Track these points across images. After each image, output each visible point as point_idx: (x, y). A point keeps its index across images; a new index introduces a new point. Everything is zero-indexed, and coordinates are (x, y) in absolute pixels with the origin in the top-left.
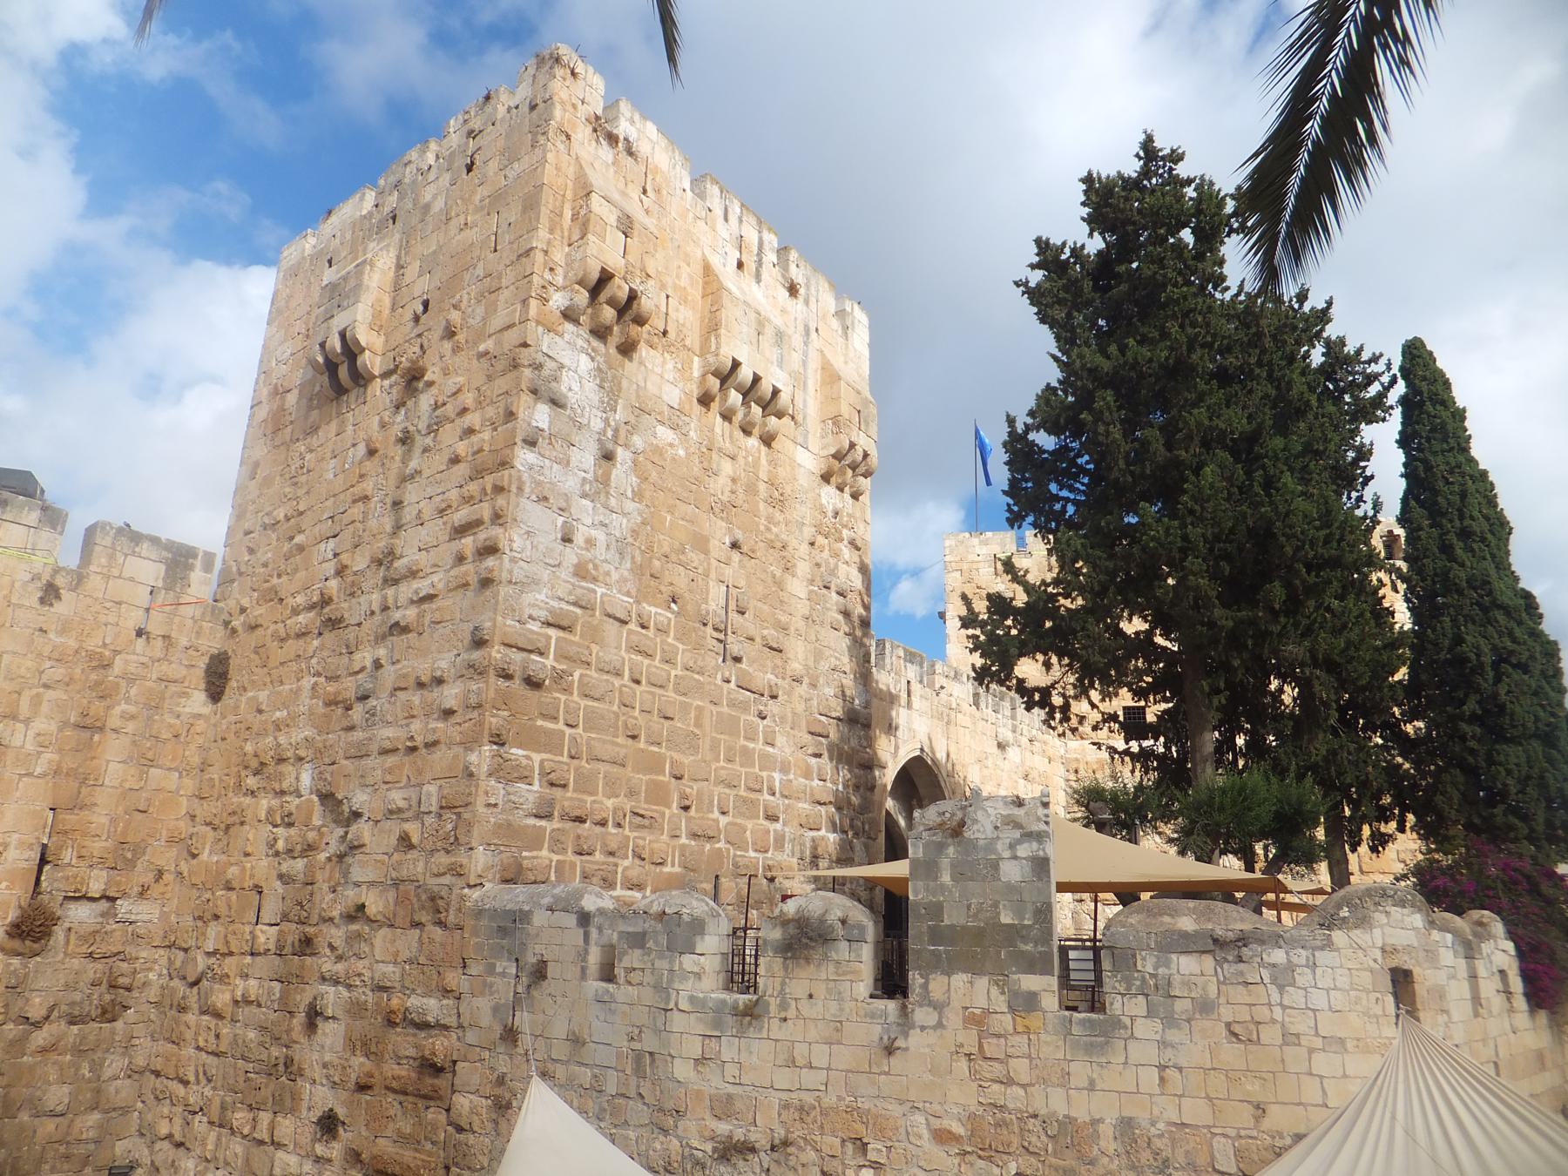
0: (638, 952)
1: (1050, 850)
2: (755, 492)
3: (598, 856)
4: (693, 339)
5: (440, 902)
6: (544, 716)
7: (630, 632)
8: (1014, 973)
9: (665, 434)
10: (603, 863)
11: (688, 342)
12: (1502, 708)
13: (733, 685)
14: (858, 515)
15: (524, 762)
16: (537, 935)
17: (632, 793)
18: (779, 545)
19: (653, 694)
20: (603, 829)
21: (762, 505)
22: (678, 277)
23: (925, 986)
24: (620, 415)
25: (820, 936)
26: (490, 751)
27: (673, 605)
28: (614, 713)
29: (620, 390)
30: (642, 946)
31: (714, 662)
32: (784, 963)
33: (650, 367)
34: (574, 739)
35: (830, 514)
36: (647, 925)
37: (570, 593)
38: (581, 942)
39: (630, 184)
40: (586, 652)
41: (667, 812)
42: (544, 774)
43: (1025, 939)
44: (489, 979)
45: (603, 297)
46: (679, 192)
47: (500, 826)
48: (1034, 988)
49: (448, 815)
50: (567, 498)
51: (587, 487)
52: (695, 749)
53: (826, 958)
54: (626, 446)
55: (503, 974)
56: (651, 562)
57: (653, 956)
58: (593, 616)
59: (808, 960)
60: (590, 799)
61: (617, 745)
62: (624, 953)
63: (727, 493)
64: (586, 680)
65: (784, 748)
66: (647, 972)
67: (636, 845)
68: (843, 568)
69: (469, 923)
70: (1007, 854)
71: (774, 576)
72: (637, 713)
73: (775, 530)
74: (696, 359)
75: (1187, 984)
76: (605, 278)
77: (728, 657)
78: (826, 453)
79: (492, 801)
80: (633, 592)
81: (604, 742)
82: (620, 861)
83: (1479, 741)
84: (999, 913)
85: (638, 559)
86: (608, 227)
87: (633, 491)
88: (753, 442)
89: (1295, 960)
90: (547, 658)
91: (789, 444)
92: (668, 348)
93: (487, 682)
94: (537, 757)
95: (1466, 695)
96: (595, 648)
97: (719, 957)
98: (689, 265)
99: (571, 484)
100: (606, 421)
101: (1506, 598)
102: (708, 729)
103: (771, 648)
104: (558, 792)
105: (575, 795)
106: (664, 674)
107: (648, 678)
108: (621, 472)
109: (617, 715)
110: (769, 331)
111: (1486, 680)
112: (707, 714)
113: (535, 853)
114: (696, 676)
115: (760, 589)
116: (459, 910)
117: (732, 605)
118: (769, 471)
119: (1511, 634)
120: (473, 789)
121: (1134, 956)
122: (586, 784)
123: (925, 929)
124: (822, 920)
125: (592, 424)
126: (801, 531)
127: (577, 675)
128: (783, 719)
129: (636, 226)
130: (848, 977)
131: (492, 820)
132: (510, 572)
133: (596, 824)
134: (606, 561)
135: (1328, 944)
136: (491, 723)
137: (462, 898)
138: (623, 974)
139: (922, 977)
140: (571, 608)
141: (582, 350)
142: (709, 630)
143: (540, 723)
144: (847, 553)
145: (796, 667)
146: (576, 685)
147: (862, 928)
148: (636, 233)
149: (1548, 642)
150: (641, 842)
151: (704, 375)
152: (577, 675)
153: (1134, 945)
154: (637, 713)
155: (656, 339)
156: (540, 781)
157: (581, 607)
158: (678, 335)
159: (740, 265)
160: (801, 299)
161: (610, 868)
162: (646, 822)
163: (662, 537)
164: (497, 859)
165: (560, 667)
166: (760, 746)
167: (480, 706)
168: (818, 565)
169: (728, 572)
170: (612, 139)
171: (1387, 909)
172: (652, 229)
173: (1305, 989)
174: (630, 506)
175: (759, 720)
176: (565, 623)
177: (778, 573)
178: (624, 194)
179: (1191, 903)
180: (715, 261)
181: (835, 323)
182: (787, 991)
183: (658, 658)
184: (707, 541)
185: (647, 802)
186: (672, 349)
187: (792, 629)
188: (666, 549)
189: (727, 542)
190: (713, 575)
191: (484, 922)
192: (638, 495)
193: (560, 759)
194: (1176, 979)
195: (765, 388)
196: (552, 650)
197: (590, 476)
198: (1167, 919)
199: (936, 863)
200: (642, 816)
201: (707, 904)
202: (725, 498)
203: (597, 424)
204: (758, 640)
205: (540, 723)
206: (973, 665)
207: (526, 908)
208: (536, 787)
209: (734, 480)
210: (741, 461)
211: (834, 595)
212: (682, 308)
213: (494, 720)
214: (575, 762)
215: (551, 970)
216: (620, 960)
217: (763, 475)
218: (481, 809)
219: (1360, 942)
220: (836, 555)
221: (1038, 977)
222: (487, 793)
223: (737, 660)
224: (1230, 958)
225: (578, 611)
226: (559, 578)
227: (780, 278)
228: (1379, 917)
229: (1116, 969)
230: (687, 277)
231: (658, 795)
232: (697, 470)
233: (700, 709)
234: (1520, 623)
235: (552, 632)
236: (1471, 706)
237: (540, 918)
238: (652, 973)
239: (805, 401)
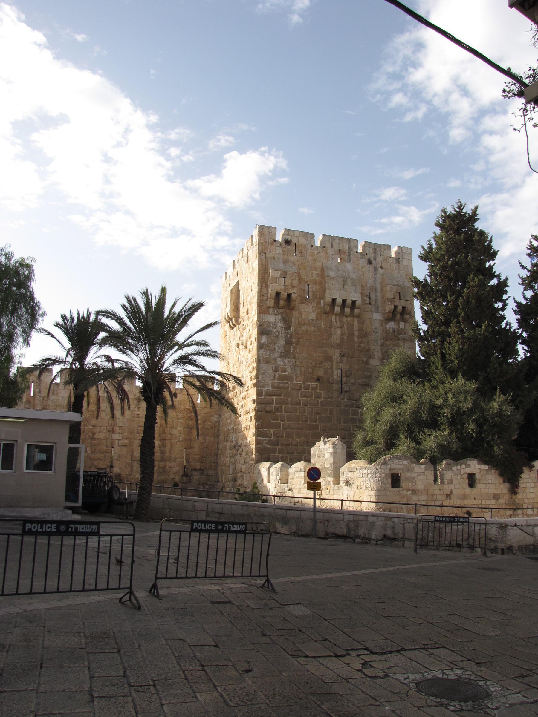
6: (273, 420)
13: (346, 400)
15: (268, 432)
20: (297, 447)
22: (312, 277)
28: (298, 415)
29: (291, 322)
42: (274, 434)
51: (282, 354)
72: (306, 414)
73: (362, 345)
80: (302, 380)
90: (273, 404)
94: (272, 431)
99: (276, 355)
103: (362, 385)
107: (310, 404)
114: (329, 400)
118: (359, 326)
142: (334, 385)
143: (272, 422)
151: (324, 305)
152: (283, 407)
154: (306, 414)
158: (313, 296)
163: (312, 361)
165: (276, 406)
183: (313, 397)
184: (332, 357)
188: (314, 364)
190: (334, 368)
195: (349, 302)
200: (311, 442)
205: (272, 422)
210: (345, 327)
217: (356, 328)
223: (346, 392)
235: (273, 397)
239: (376, 296)
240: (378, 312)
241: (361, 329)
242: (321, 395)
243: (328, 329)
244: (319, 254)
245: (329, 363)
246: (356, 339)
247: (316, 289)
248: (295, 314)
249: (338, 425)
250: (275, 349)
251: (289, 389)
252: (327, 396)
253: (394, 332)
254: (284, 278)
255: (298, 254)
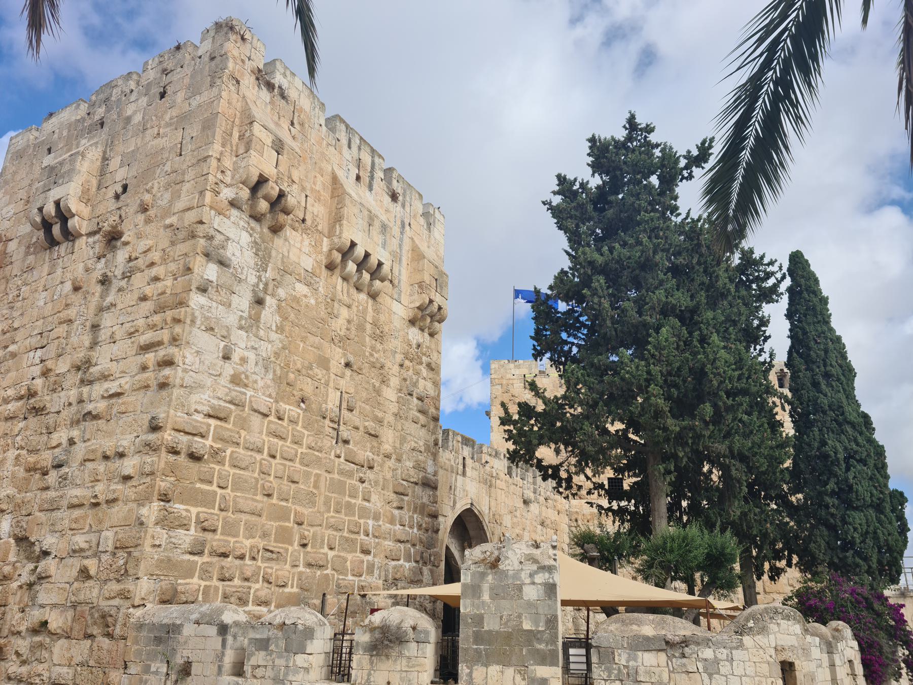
0: (263, 653)
1: (557, 578)
2: (364, 330)
3: (237, 582)
4: (323, 226)
5: (110, 619)
6: (202, 481)
7: (270, 422)
8: (532, 665)
9: (301, 289)
10: (240, 587)
11: (320, 228)
12: (850, 487)
13: (342, 460)
14: (433, 347)
15: (184, 514)
16: (186, 642)
17: (265, 535)
18: (378, 365)
19: (284, 465)
20: (242, 562)
21: (368, 339)
22: (314, 183)
23: (470, 675)
24: (270, 274)
25: (397, 639)
26: (158, 506)
27: (302, 404)
28: (255, 478)
29: (270, 257)
30: (266, 648)
31: (329, 444)
32: (370, 660)
33: (292, 243)
34: (224, 497)
35: (414, 346)
36: (270, 633)
37: (227, 395)
38: (219, 647)
39: (282, 119)
40: (237, 436)
41: (290, 548)
42: (199, 522)
43: (539, 641)
44: (144, 677)
45: (260, 194)
46: (317, 126)
47: (162, 561)
48: (545, 676)
49: (121, 554)
50: (228, 329)
51: (243, 322)
52: (313, 503)
53: (401, 654)
54: (273, 295)
55: (156, 673)
56: (287, 375)
57: (274, 656)
58: (244, 410)
59: (387, 657)
60: (232, 540)
61: (257, 501)
62: (252, 654)
63: (344, 330)
64: (235, 455)
65: (377, 503)
66: (269, 668)
67: (265, 573)
68: (422, 383)
69: (132, 634)
70: (528, 581)
71: (374, 386)
72: (272, 478)
73: (376, 355)
74: (325, 239)
75: (648, 673)
76: (262, 181)
77: (340, 440)
78: (412, 306)
79: (157, 543)
80: (274, 395)
81: (246, 499)
82: (253, 585)
83: (837, 509)
84: (522, 622)
85: (278, 372)
86: (266, 147)
87: (277, 326)
88: (363, 297)
89: (719, 656)
90: (208, 439)
91: (388, 298)
92: (305, 231)
93: (159, 457)
94: (194, 510)
95: (829, 479)
96: (243, 433)
97: (323, 656)
98: (322, 176)
99: (231, 319)
100: (259, 278)
101: (853, 417)
102: (323, 490)
103: (370, 434)
104: (209, 536)
105: (222, 537)
106: (293, 451)
107: (281, 454)
108: (269, 315)
109: (257, 480)
110: (377, 224)
111: (840, 469)
112: (322, 479)
113: (188, 581)
114: (316, 453)
115: (364, 394)
116: (125, 625)
117: (344, 405)
119: (856, 441)
120: (143, 534)
121: (613, 653)
122: (230, 529)
123: (470, 633)
124: (399, 628)
125: (249, 279)
126: (394, 357)
127: (228, 452)
128: (376, 483)
129: (286, 147)
130: (416, 669)
131: (156, 557)
132: (183, 379)
133: (236, 558)
134: (255, 373)
135: (740, 646)
136: (160, 486)
137: (128, 616)
138: (250, 671)
139: (468, 667)
140: (228, 405)
141: (244, 228)
142: (327, 422)
143: (198, 485)
144: (424, 372)
145: (387, 447)
146: (228, 459)
147: (427, 633)
148: (285, 152)
149: (879, 446)
150: (269, 571)
151: (330, 251)
152: (228, 452)
153: (613, 645)
154: (272, 478)
155: (297, 224)
156: (196, 527)
157: (235, 404)
158: (313, 222)
159: (358, 178)
160: (400, 203)
161: (245, 590)
162: (274, 556)
163: (296, 358)
164: (157, 586)
165: (216, 446)
166: (359, 501)
167: (152, 473)
168: (405, 380)
169: (342, 383)
170: (270, 86)
171: (779, 621)
172: (297, 150)
173: (726, 676)
174: (274, 336)
175: (360, 484)
176: (222, 415)
177: (377, 385)
178: (277, 124)
179: (651, 617)
180: (341, 174)
181: (422, 221)
182: (372, 679)
183: (289, 440)
185: (276, 541)
186: (308, 231)
187: (386, 422)
188: (299, 366)
189: (343, 362)
190: (331, 384)
191: (144, 633)
192: (280, 329)
193: (212, 511)
194: (641, 670)
195: (373, 261)
196: (211, 434)
197: (246, 315)
198: (635, 627)
199: (479, 586)
200: (272, 552)
201: (317, 617)
202: (342, 333)
203: (252, 280)
204: (361, 429)
205: (198, 485)
206: (508, 449)
207: (178, 622)
208: (192, 531)
209: (349, 322)
210: (354, 309)
211: (415, 399)
212: (316, 204)
213: (163, 484)
214: (224, 513)
215: (194, 670)
216: (249, 660)
217: (369, 319)
218: (148, 548)
219: (761, 644)
220: (418, 373)
221: (548, 667)
222: (153, 537)
223: (346, 442)
224: (677, 655)
225: (233, 407)
226: (219, 384)
227: (385, 189)
228: (773, 627)
229: (600, 663)
230: (321, 183)
231: (284, 536)
232: (323, 314)
233: (318, 476)
234: (861, 433)
235: (212, 422)
236: (831, 486)
237: (189, 630)
238: (273, 669)
240: (400, 302)
241: (375, 324)
242: (303, 438)
243: (329, 300)
244: (330, 147)
245: (324, 372)
246: (368, 339)
247: (318, 211)
248: (278, 242)
249: (325, 516)
250: (230, 305)
251: (246, 409)
252: (313, 445)
253: (419, 346)
254: (278, 154)
255: (296, 125)
